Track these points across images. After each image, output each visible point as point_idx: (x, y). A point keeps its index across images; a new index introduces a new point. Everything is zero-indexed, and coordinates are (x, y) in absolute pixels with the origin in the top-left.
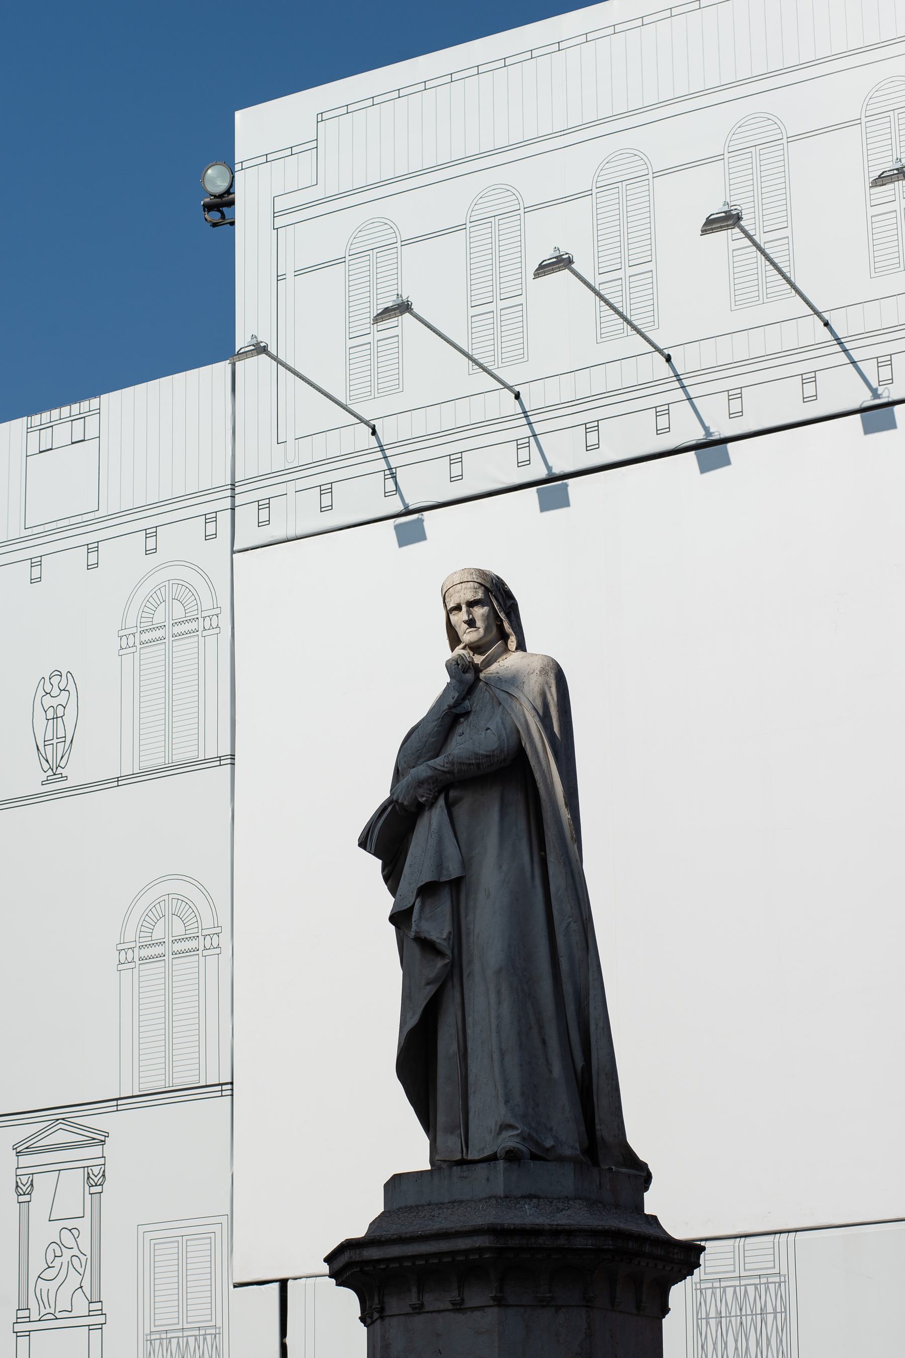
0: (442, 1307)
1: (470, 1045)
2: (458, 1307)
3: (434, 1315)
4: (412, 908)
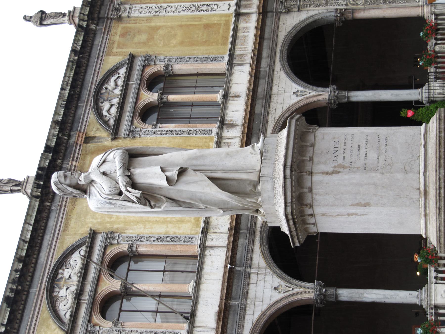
0: (312, 151)
1: (220, 168)
2: (313, 145)
3: (314, 154)
4: (167, 177)
